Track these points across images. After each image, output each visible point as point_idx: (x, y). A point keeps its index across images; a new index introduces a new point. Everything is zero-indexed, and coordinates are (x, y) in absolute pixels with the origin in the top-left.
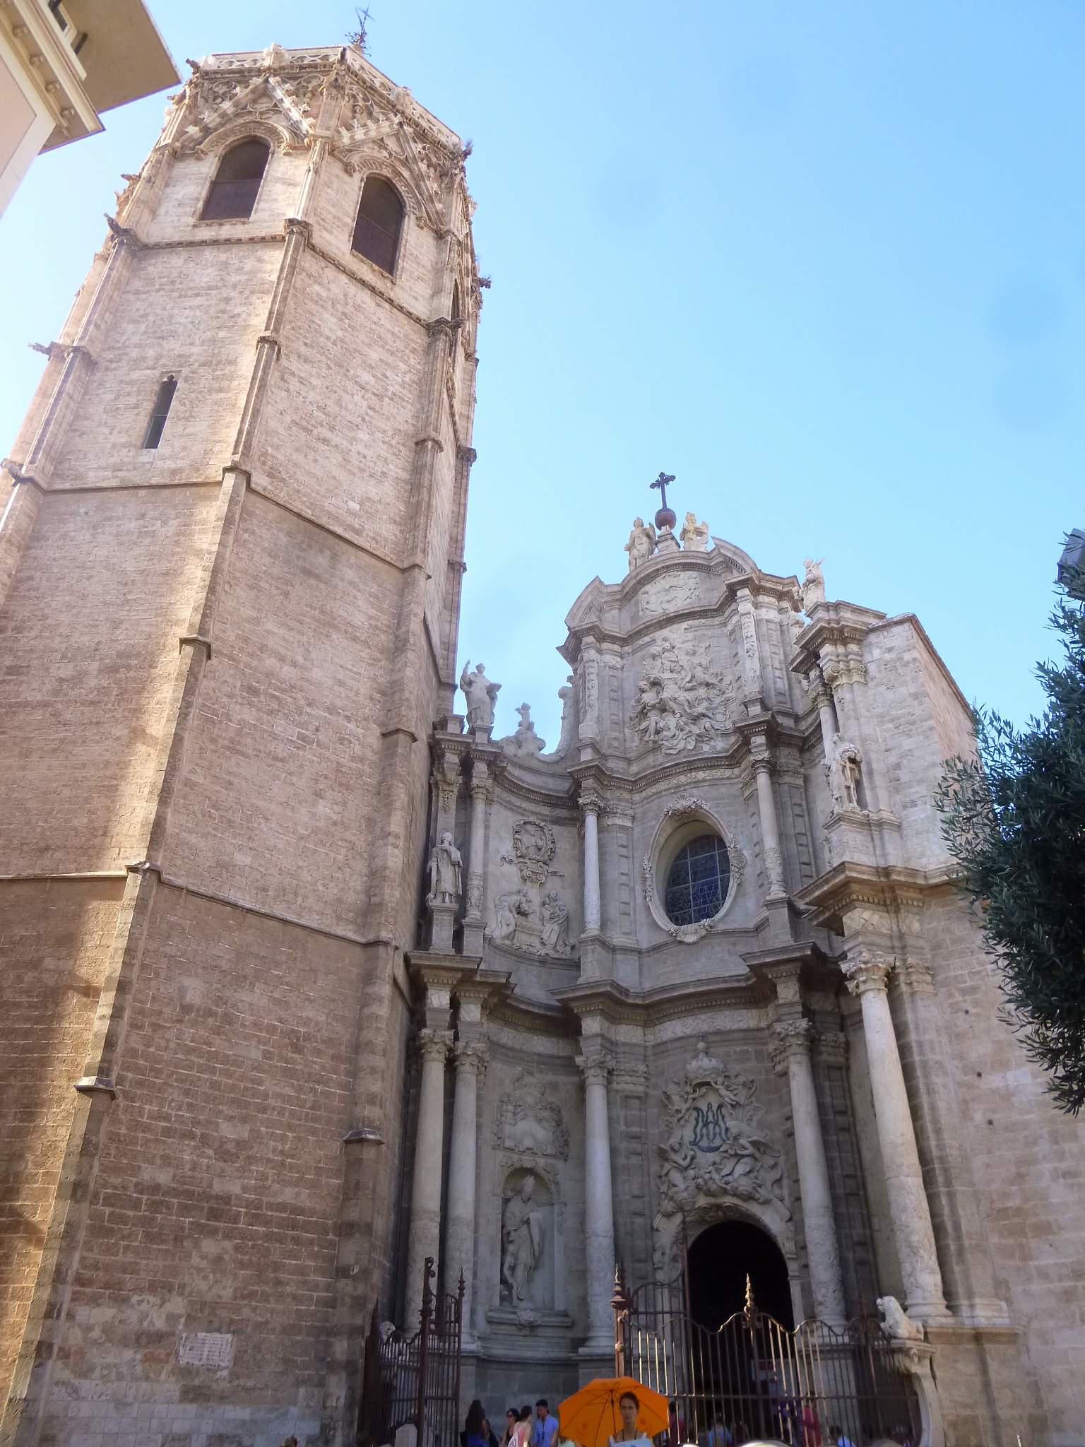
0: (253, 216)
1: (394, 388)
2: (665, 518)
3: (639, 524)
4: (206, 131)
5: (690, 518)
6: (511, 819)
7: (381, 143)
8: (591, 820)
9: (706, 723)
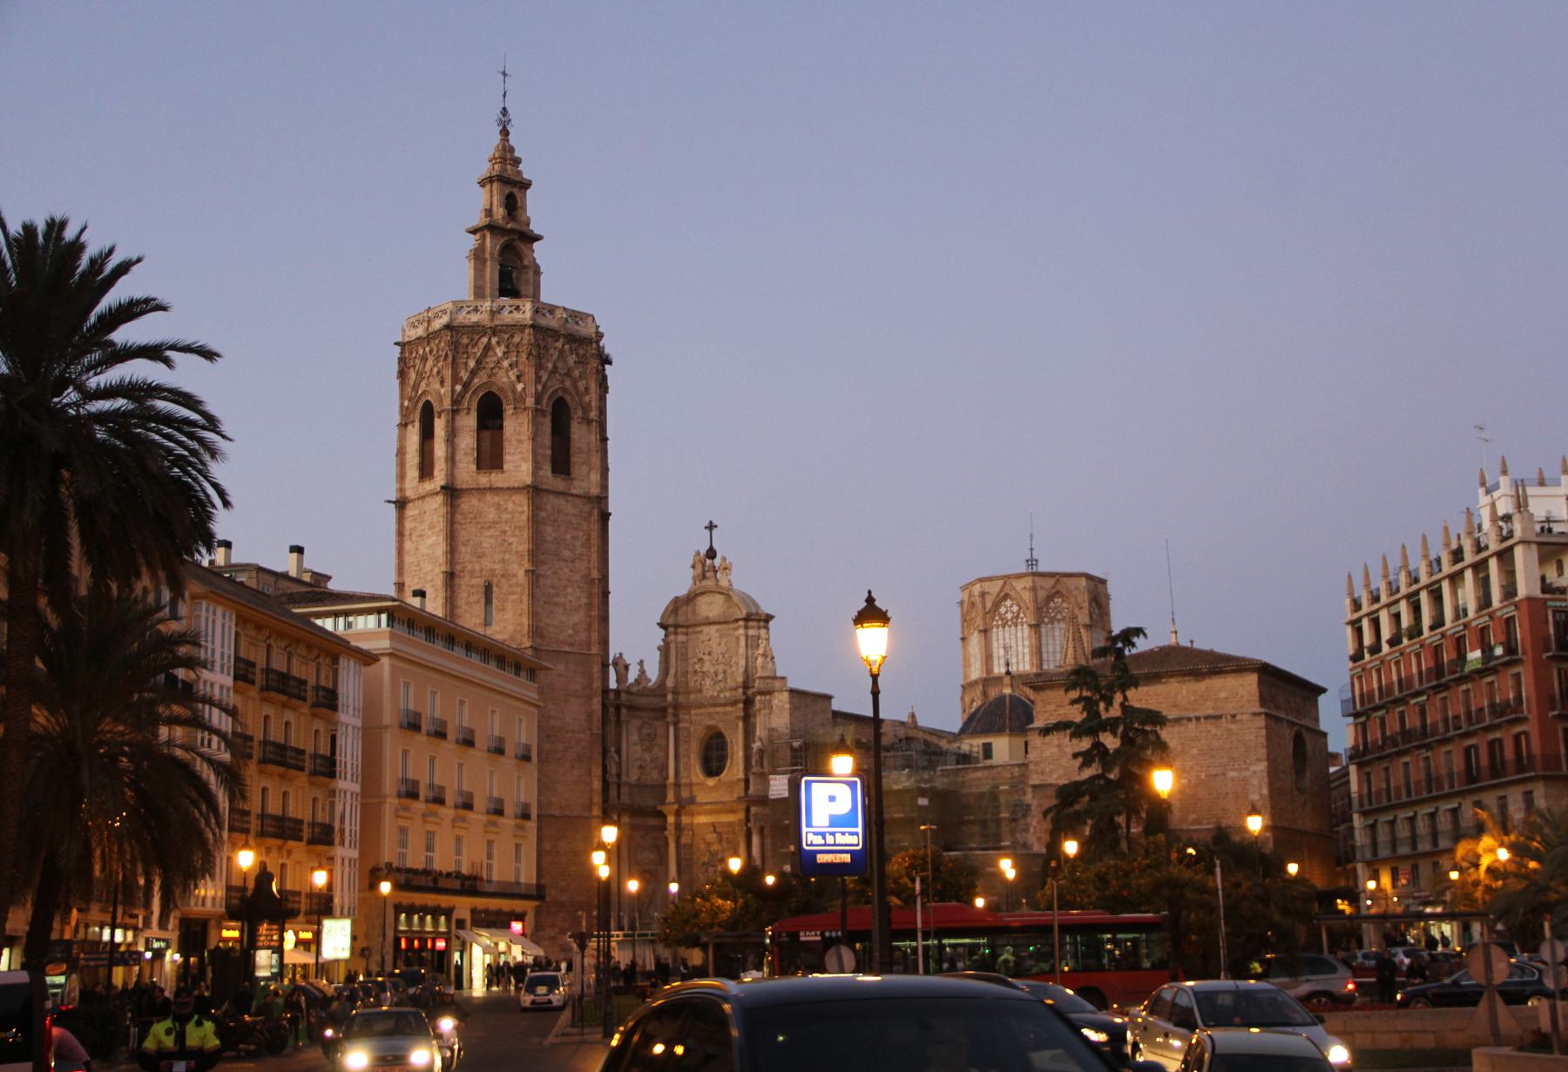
0: (506, 467)
1: (579, 550)
2: (711, 553)
3: (698, 553)
4: (466, 386)
5: (724, 559)
6: (638, 722)
7: (555, 370)
8: (671, 729)
9: (722, 685)
